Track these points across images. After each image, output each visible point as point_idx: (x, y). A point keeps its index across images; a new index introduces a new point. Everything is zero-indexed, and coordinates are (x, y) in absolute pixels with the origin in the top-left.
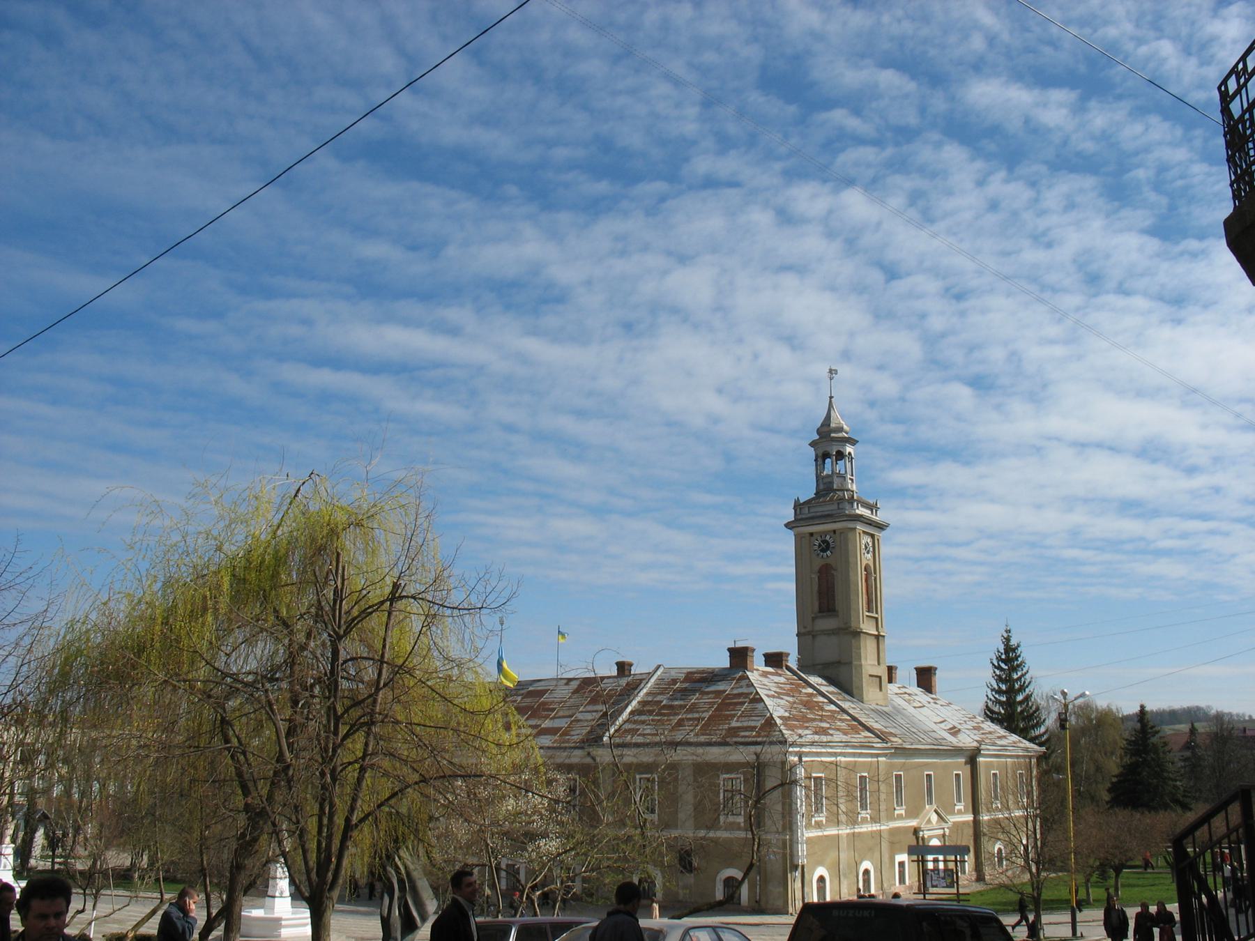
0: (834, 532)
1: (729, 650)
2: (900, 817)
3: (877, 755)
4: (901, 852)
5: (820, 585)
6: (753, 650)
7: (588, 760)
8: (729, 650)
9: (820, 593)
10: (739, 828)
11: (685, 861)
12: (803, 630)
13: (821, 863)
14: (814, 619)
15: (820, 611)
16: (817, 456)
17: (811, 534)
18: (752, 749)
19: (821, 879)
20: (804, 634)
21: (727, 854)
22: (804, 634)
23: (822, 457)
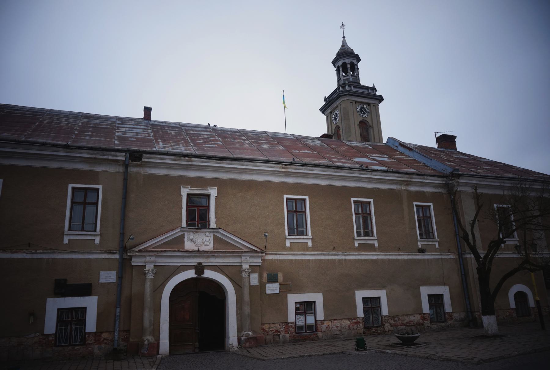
0: (369, 104)
17: (356, 102)
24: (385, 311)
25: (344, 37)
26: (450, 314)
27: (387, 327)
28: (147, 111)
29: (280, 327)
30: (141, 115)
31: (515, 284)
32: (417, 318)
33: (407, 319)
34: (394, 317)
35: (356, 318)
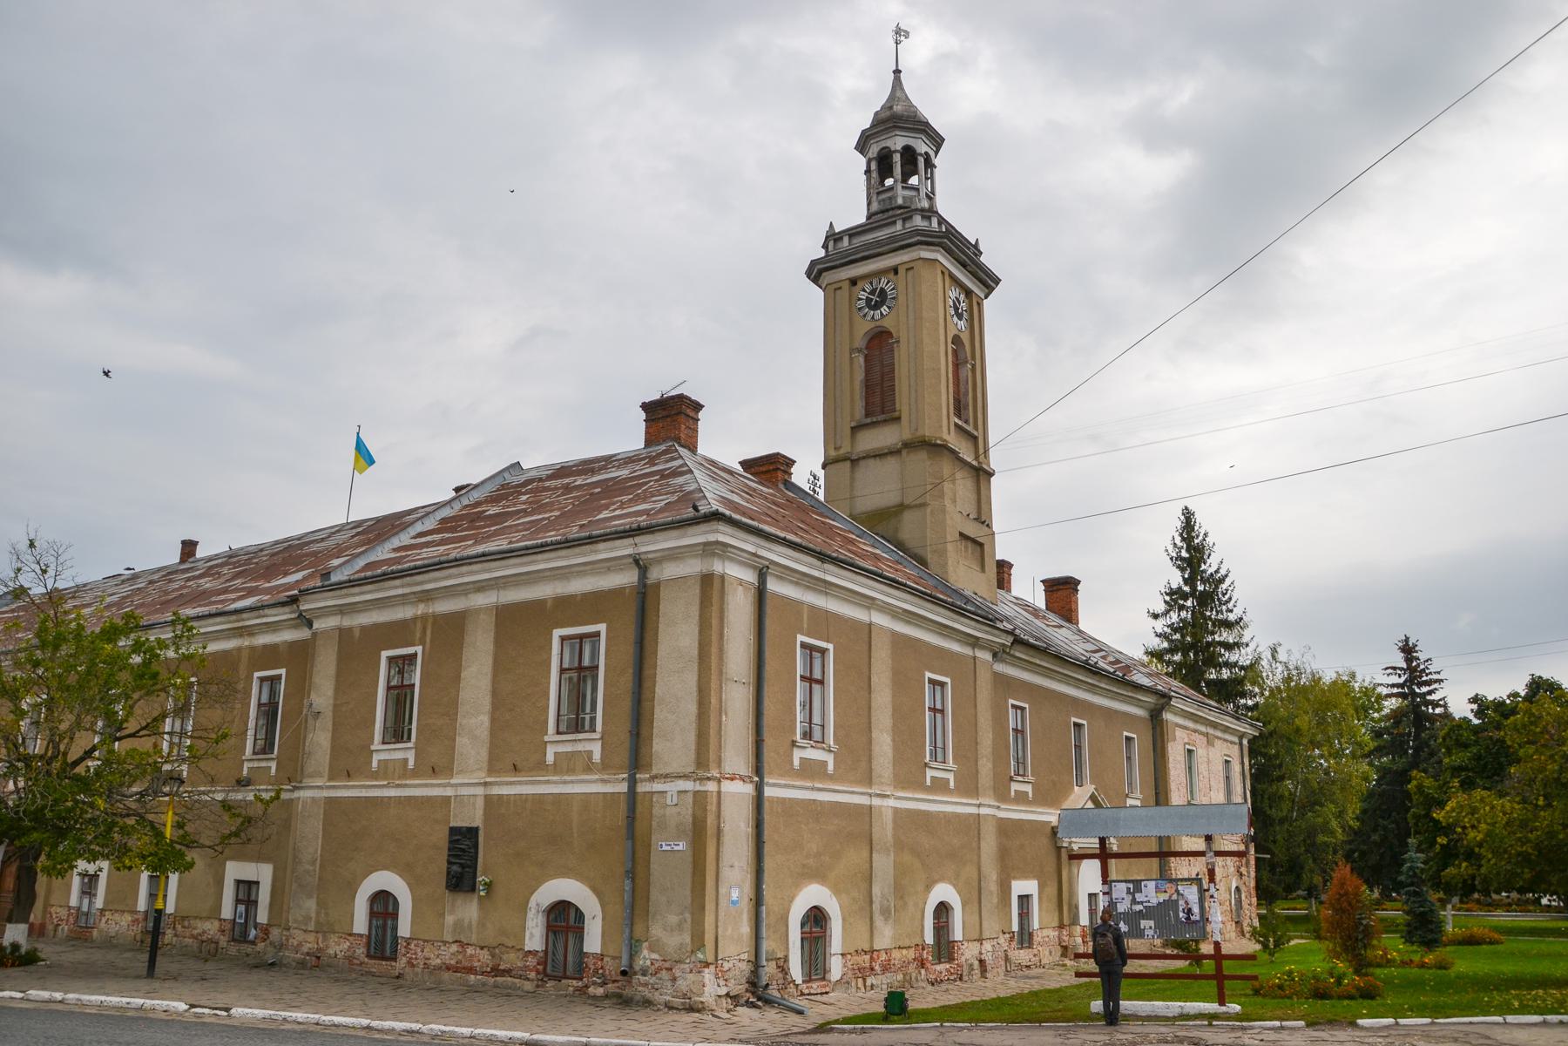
0: (895, 270)
1: (645, 406)
2: (1021, 798)
3: (974, 642)
4: (1025, 875)
5: (867, 372)
6: (698, 407)
7: (303, 634)
8: (645, 406)
9: (868, 386)
10: (589, 767)
11: (462, 860)
12: (833, 453)
13: (818, 875)
15: (867, 415)
17: (853, 282)
18: (624, 548)
20: (836, 461)
22: (836, 461)
23: (882, 165)
25: (897, 72)
34: (183, 918)
35: (136, 912)
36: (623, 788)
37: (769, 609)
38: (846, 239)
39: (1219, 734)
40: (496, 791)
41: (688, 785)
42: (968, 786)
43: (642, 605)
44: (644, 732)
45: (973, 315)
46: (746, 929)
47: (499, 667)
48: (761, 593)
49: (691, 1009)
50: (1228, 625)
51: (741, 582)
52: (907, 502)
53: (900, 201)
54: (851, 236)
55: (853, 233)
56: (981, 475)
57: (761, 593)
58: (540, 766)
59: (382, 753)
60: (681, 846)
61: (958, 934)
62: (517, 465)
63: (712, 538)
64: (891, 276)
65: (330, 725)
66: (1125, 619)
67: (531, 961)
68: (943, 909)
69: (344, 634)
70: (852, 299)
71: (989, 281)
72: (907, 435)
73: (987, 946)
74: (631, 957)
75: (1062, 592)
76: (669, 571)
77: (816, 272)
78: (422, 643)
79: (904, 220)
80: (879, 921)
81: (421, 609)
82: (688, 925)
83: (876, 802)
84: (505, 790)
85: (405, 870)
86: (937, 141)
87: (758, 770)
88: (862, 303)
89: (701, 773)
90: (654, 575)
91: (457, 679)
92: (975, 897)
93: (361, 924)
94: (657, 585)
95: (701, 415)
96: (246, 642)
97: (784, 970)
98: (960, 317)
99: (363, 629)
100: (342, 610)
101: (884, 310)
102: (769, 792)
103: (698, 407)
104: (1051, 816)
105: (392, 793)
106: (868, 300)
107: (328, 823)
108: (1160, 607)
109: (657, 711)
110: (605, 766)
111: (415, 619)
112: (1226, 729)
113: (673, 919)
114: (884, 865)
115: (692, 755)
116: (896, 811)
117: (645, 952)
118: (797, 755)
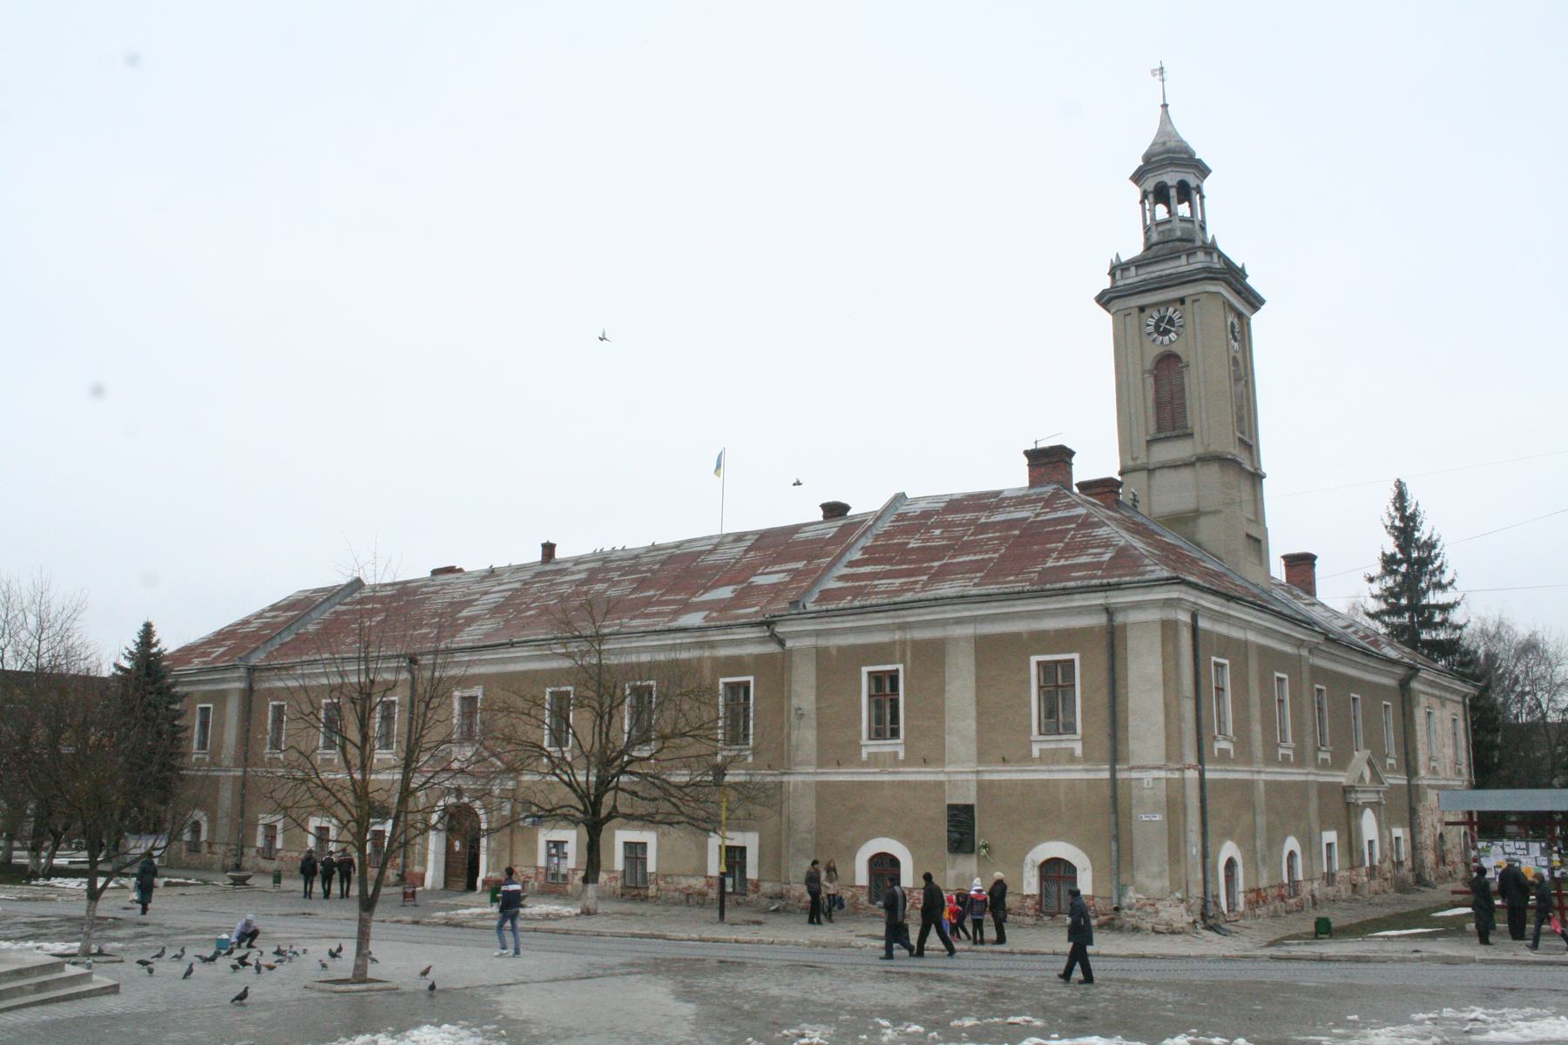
0: (1182, 301)
1: (1027, 453)
3: (1300, 643)
4: (1329, 829)
6: (1071, 453)
8: (1027, 453)
9: (1159, 405)
10: (1072, 759)
11: (961, 829)
12: (1130, 463)
14: (1150, 443)
15: (1159, 429)
16: (1145, 196)
17: (1142, 309)
18: (1097, 599)
19: (1231, 864)
21: (1042, 810)
24: (651, 867)
25: (1165, 106)
26: (756, 885)
27: (652, 890)
28: (548, 549)
29: (531, 872)
30: (537, 556)
31: (885, 836)
32: (698, 883)
33: (684, 882)
36: (1106, 775)
37: (1201, 642)
38: (1133, 269)
39: (1448, 696)
40: (987, 777)
41: (1162, 774)
42: (1300, 762)
43: (1113, 640)
44: (1119, 735)
45: (1241, 333)
46: (1200, 876)
47: (981, 684)
48: (1195, 629)
49: (1173, 932)
50: (1440, 586)
51: (1185, 624)
52: (1205, 507)
53: (1178, 234)
54: (1137, 267)
55: (1138, 263)
56: (1256, 477)
57: (1195, 629)
58: (1027, 758)
59: (869, 747)
60: (1158, 817)
61: (1300, 876)
62: (900, 498)
63: (1174, 595)
64: (1178, 306)
65: (814, 724)
66: (1349, 588)
67: (1029, 902)
68: (1292, 854)
69: (821, 654)
70: (1142, 325)
71: (1255, 302)
72: (1200, 450)
73: (1316, 885)
74: (1119, 897)
75: (1301, 565)
76: (1133, 617)
77: (1105, 300)
78: (902, 661)
79: (1188, 255)
80: (1261, 868)
81: (897, 636)
82: (1167, 874)
83: (1256, 777)
84: (995, 777)
85: (905, 838)
86: (1203, 171)
87: (1201, 761)
88: (1151, 329)
89: (1171, 765)
90: (1119, 619)
91: (941, 691)
92: (1308, 843)
93: (862, 877)
94: (1125, 625)
95: (1074, 460)
96: (707, 653)
97: (1217, 904)
98: (1235, 339)
99: (839, 648)
100: (818, 633)
101: (1173, 336)
102: (1208, 775)
103: (1071, 453)
104: (1342, 778)
105: (886, 778)
106: (1157, 327)
107: (820, 800)
108: (1377, 569)
109: (1131, 719)
110: (1086, 758)
111: (894, 643)
112: (1454, 691)
113: (1155, 869)
114: (1261, 821)
115: (1162, 752)
116: (1266, 783)
117: (1131, 894)
118: (1217, 745)
